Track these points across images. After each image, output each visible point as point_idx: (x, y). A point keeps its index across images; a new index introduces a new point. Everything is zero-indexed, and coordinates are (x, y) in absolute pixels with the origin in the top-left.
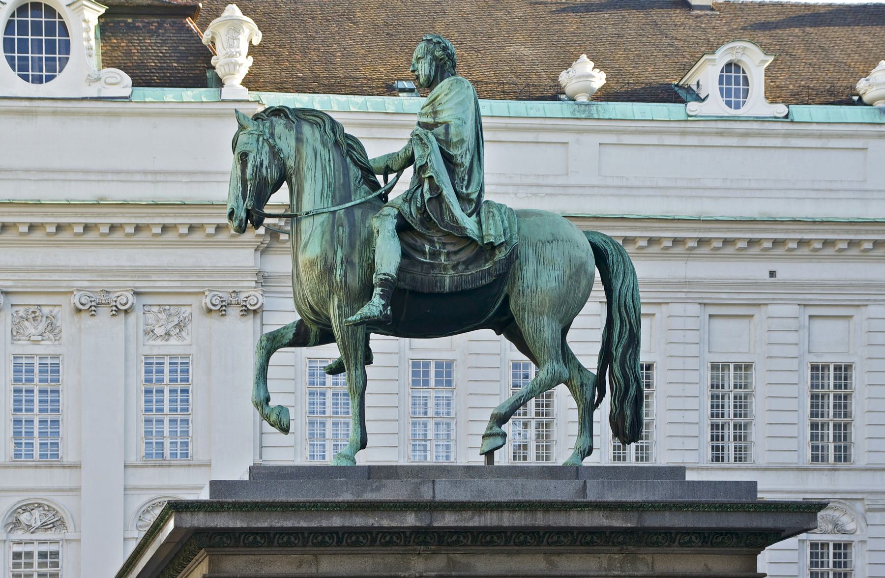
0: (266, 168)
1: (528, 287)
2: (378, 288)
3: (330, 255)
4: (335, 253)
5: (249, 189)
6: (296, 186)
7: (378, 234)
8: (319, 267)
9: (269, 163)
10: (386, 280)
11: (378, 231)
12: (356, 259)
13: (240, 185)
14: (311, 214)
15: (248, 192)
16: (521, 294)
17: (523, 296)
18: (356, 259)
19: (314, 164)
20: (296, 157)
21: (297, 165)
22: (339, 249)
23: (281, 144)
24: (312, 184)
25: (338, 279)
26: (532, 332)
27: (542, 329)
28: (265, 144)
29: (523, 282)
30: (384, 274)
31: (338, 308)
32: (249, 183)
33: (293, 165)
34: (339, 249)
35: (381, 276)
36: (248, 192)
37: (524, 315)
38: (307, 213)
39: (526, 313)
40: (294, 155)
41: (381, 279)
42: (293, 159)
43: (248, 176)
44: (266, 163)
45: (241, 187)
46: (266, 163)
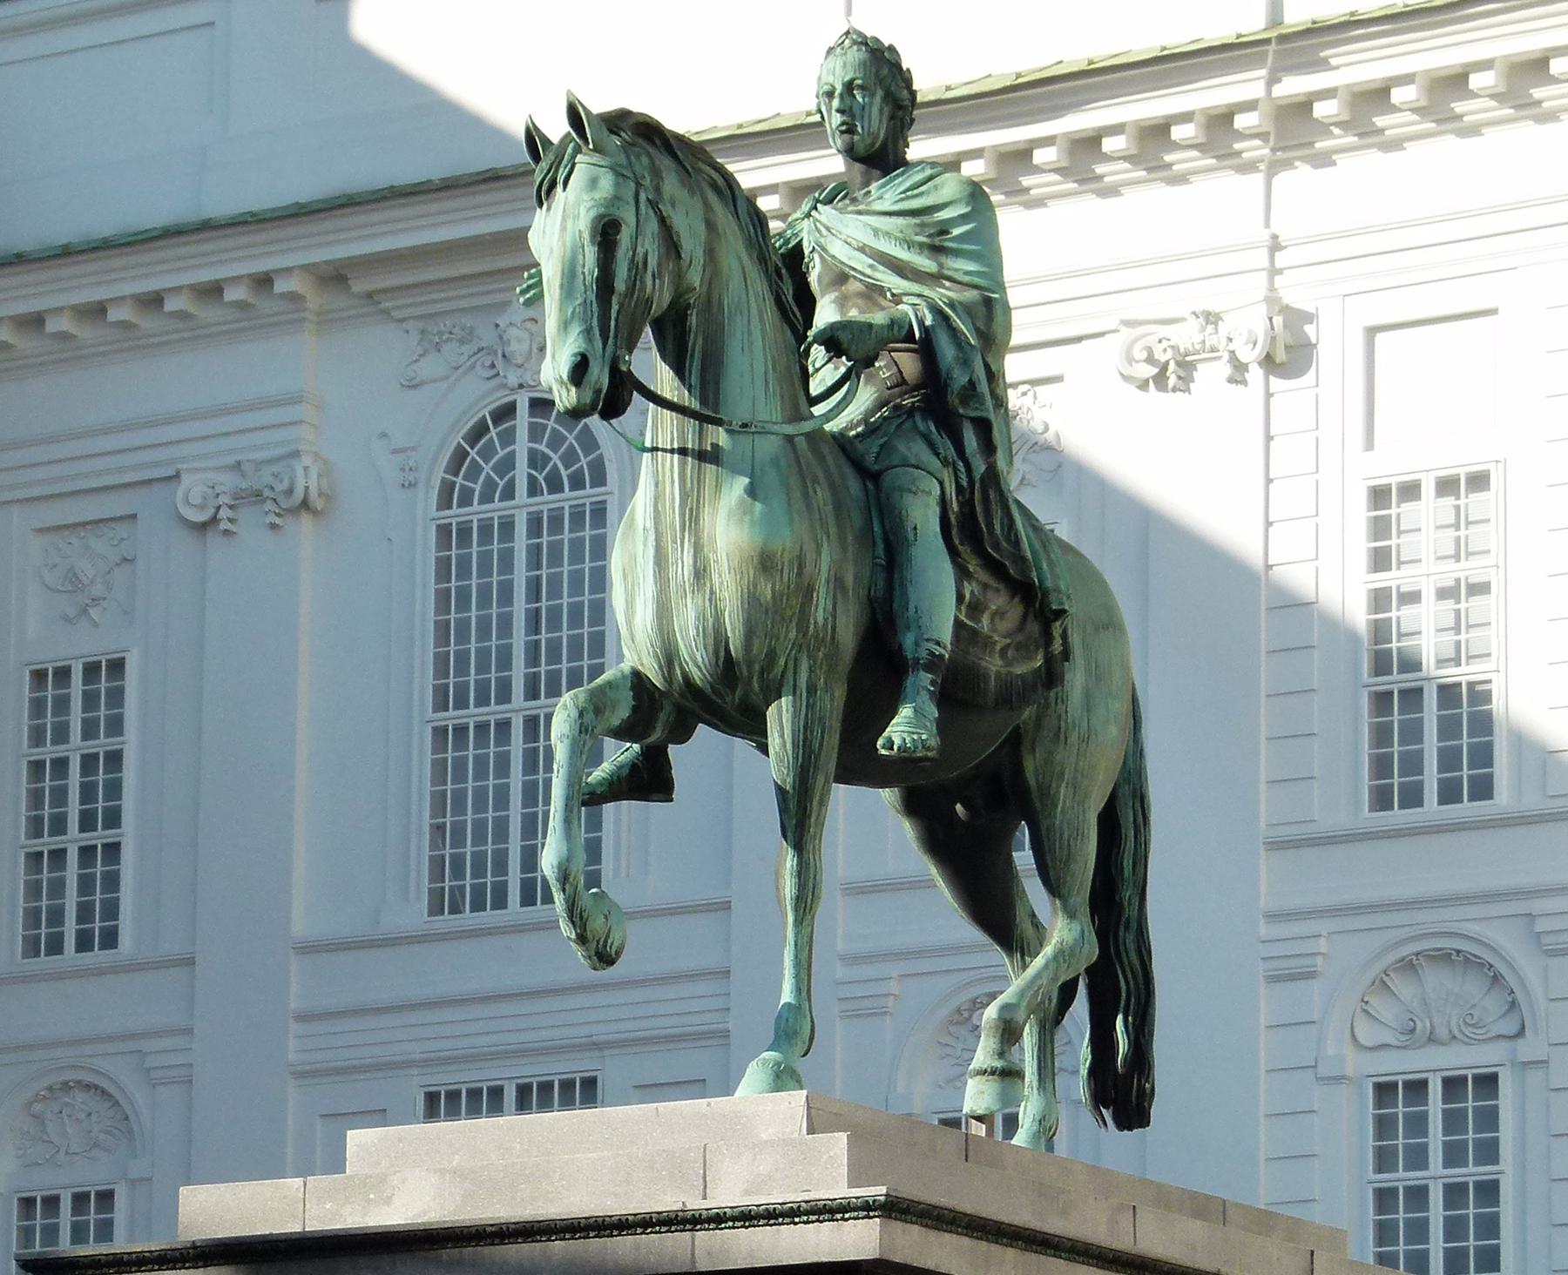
0: (653, 275)
1: (1074, 723)
3: (810, 557)
4: (819, 553)
5: (613, 315)
6: (700, 341)
7: (916, 534)
8: (786, 579)
9: (659, 265)
10: (941, 656)
11: (915, 528)
14: (753, 429)
15: (613, 323)
16: (1062, 736)
17: (1066, 744)
18: (849, 579)
19: (744, 297)
20: (704, 267)
21: (705, 288)
22: (825, 545)
23: (679, 222)
24: (746, 348)
25: (820, 620)
26: (1069, 836)
27: (1086, 831)
28: (651, 212)
29: (1066, 712)
30: (938, 643)
31: (808, 692)
32: (615, 300)
33: (697, 285)
34: (825, 545)
36: (613, 323)
37: (1059, 787)
38: (745, 425)
39: (1063, 785)
40: (702, 262)
41: (932, 654)
42: (700, 268)
43: (620, 285)
44: (652, 262)
45: (595, 305)
46: (652, 262)
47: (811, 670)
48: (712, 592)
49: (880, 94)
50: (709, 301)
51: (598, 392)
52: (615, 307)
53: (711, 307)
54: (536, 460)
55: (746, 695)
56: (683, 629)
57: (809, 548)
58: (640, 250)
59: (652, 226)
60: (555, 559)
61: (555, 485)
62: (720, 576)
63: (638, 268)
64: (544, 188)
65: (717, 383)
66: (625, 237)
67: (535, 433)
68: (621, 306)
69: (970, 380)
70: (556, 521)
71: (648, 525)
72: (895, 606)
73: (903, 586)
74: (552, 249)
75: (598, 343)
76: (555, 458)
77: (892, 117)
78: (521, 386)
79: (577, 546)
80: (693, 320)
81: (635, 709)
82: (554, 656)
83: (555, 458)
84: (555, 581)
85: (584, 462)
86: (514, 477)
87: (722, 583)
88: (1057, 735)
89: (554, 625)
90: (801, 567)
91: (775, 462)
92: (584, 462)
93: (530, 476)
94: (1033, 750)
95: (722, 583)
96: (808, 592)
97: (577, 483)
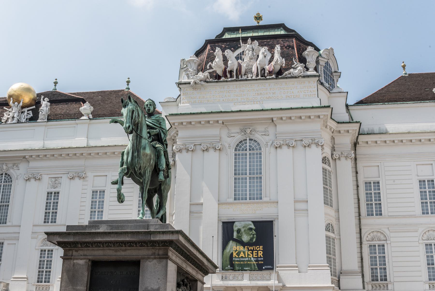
2: (162, 172)
3: (151, 155)
4: (152, 155)
12: (154, 159)
13: (130, 119)
18: (154, 159)
32: (133, 120)
35: (163, 168)
38: (145, 138)
44: (137, 116)
46: (137, 116)
47: (150, 169)
48: (139, 158)
49: (153, 106)
50: (141, 123)
51: (131, 130)
52: (133, 121)
53: (141, 124)
54: (5, 179)
55: (141, 171)
56: (135, 162)
57: (151, 154)
58: (136, 115)
59: (137, 112)
60: (6, 189)
61: (6, 182)
62: (141, 156)
63: (135, 116)
64: (125, 105)
65: (142, 133)
66: (135, 112)
67: (5, 177)
68: (133, 120)
69: (165, 139)
70: (6, 186)
71: (131, 149)
72: (158, 163)
73: (160, 161)
74: (125, 112)
75: (131, 124)
76: (7, 179)
77: (154, 109)
78: (4, 172)
79: (8, 188)
80: (139, 125)
81: (127, 171)
82: (4, 199)
83: (7, 179)
84: (5, 192)
85: (10, 180)
86: (2, 181)
87: (141, 157)
88: (166, 184)
89: (5, 196)
90: (150, 156)
91: (147, 143)
92: (10, 180)
93: (4, 181)
94: (163, 185)
95: (141, 157)
96: (151, 159)
97: (9, 182)
